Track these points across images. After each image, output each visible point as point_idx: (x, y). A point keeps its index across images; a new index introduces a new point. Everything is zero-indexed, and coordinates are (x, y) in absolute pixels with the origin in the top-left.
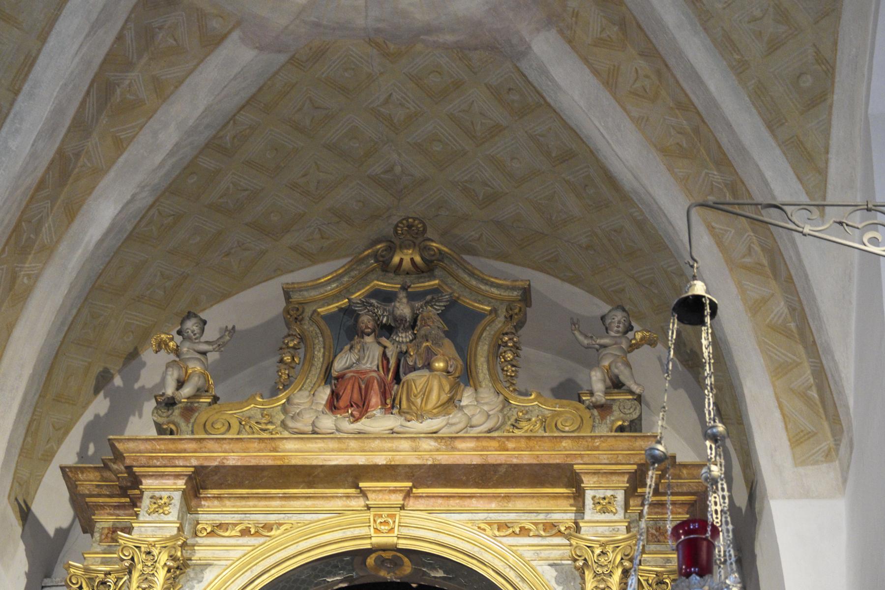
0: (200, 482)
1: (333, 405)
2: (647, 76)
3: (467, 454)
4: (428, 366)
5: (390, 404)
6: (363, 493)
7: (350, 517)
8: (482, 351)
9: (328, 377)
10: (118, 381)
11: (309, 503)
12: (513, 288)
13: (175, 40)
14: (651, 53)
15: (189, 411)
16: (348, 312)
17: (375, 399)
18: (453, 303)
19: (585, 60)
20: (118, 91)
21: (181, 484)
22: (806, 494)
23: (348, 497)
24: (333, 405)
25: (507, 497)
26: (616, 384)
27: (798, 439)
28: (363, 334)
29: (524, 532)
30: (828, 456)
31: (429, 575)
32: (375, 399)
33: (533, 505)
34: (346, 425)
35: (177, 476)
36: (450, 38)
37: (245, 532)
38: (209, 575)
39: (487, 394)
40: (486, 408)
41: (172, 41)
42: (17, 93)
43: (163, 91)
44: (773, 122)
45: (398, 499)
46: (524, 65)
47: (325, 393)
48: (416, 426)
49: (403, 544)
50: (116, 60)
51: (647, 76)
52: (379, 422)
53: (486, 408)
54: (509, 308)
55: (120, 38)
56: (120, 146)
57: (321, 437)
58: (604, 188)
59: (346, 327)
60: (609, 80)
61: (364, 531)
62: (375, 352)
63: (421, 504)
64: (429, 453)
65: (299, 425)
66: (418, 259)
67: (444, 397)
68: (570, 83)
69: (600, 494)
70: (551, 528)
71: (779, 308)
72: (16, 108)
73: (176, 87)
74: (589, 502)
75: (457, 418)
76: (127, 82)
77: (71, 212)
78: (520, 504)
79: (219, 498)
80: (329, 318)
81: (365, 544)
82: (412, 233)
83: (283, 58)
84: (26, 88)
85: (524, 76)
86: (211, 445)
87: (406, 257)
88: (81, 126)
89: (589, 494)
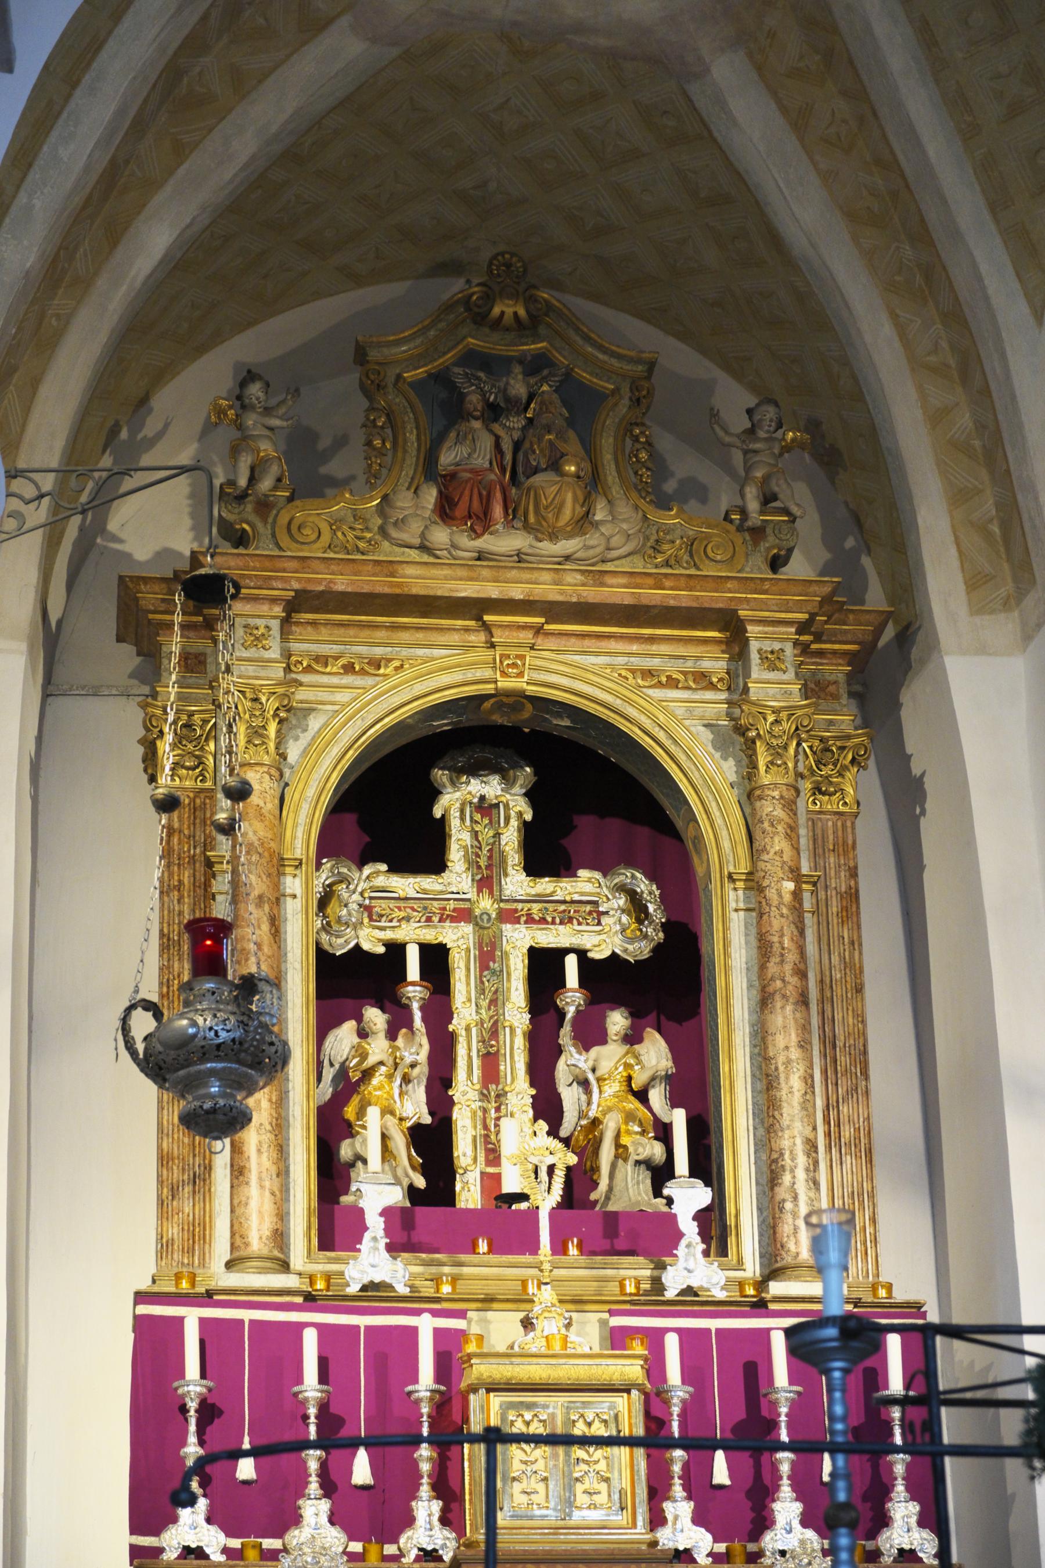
0: (299, 605)
1: (445, 511)
2: (844, 121)
3: (617, 592)
4: (555, 466)
5: (514, 513)
6: (487, 628)
7: (471, 656)
8: (607, 444)
9: (429, 469)
10: (124, 434)
11: (420, 635)
12: (639, 361)
13: (266, 19)
14: (858, 94)
15: (264, 507)
16: (441, 378)
17: (498, 511)
18: (568, 375)
19: (774, 93)
20: (185, 80)
21: (278, 610)
22: (982, 650)
23: (467, 630)
24: (445, 511)
25: (652, 639)
26: (768, 499)
27: (976, 582)
28: (468, 416)
29: (672, 683)
30: (1006, 605)
31: (550, 722)
32: (498, 511)
33: (681, 650)
34: (464, 540)
35: (274, 600)
36: (603, 42)
37: (349, 669)
38: (315, 723)
39: (624, 509)
40: (625, 526)
41: (261, 21)
42: (74, 85)
43: (242, 84)
44: (998, 203)
45: (527, 636)
46: (694, 89)
47: (430, 495)
48: (547, 547)
49: (531, 690)
50: (194, 44)
51: (844, 121)
52: (506, 541)
53: (625, 526)
54: (635, 387)
55: (205, 18)
56: (180, 151)
57: (443, 562)
58: (759, 240)
59: (447, 406)
60: (799, 121)
61: (488, 673)
62: (486, 442)
63: (552, 643)
64: (572, 588)
65: (405, 537)
66: (522, 312)
67: (580, 511)
68: (750, 121)
69: (767, 646)
70: (703, 681)
71: (964, 420)
72: (72, 105)
73: (260, 82)
74: (754, 657)
75: (593, 539)
76: (198, 69)
77: (115, 234)
78: (665, 648)
79: (314, 624)
80: (417, 386)
81: (489, 689)
82: (510, 274)
83: (395, 52)
84: (87, 79)
85: (691, 101)
86: (315, 564)
87: (506, 308)
88: (139, 127)
89: (754, 646)
